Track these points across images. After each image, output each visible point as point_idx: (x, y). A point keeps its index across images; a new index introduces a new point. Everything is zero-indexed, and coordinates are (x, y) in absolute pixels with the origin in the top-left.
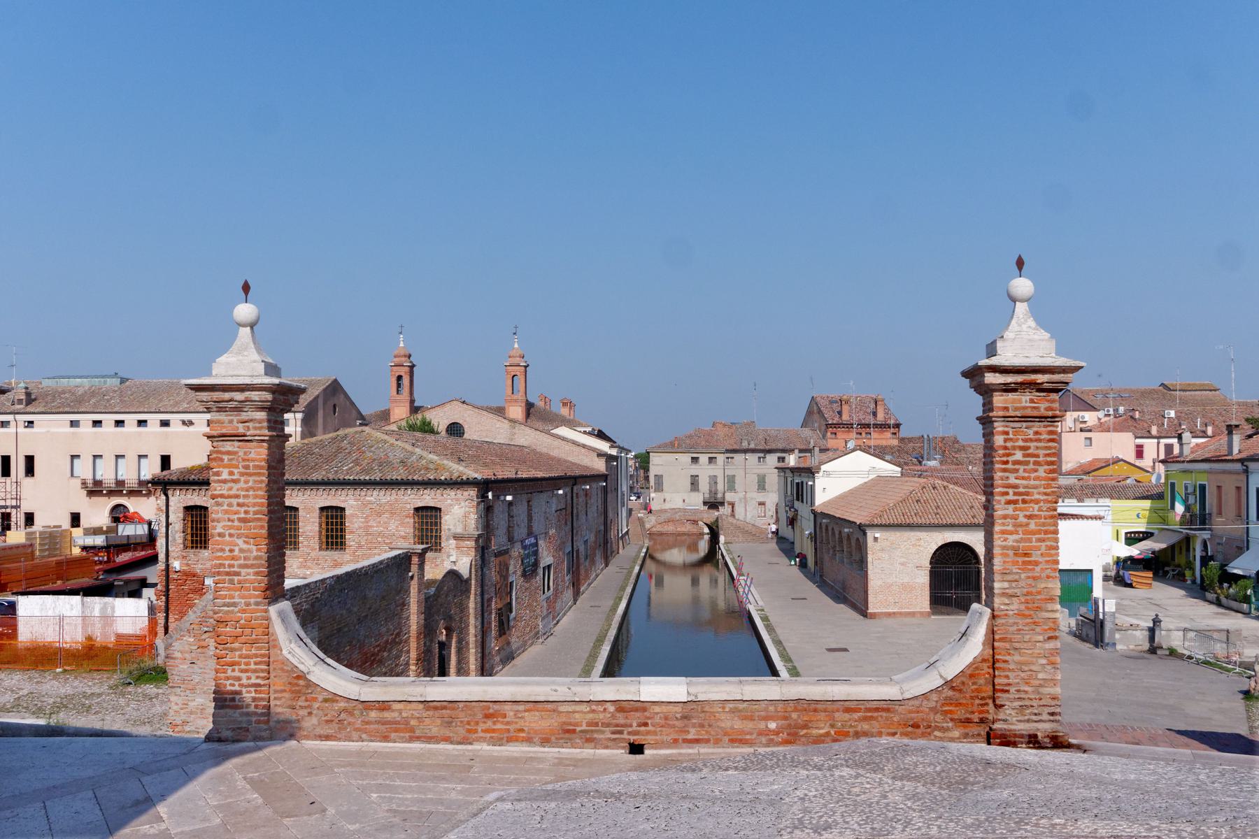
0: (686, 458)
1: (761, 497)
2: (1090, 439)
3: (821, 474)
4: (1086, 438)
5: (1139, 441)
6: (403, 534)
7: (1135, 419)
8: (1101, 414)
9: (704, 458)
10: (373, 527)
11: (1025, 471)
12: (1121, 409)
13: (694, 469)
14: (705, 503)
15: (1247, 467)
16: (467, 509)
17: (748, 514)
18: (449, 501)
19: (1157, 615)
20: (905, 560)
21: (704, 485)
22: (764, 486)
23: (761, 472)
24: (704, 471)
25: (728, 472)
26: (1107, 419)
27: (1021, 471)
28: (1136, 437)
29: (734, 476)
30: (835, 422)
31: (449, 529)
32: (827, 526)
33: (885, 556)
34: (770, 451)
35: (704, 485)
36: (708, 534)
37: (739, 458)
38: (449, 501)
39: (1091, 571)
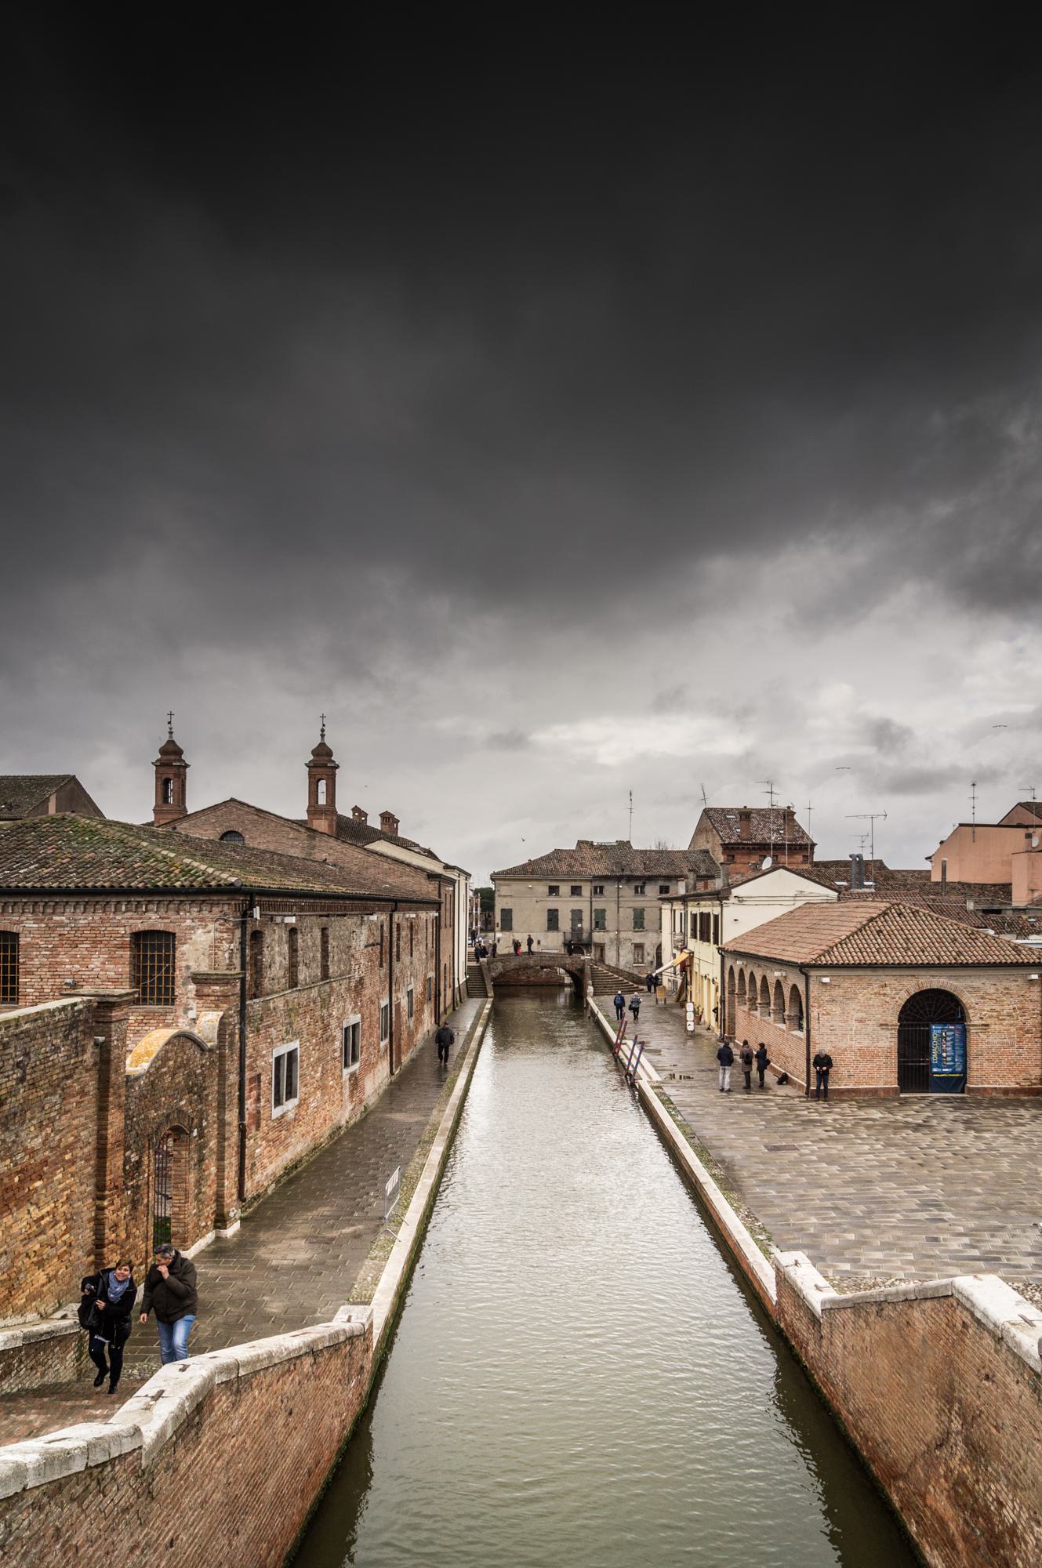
0: (542, 888)
1: (638, 938)
3: (732, 900)
6: (112, 974)
9: (565, 889)
10: (64, 964)
13: (553, 903)
16: (218, 935)
17: (621, 958)
18: (188, 922)
20: (863, 1015)
21: (565, 923)
22: (642, 923)
23: (639, 905)
24: (565, 905)
25: (596, 906)
29: (604, 910)
30: (732, 841)
31: (188, 967)
32: (741, 971)
33: (836, 1009)
35: (565, 923)
36: (569, 985)
37: (610, 888)
38: (188, 922)
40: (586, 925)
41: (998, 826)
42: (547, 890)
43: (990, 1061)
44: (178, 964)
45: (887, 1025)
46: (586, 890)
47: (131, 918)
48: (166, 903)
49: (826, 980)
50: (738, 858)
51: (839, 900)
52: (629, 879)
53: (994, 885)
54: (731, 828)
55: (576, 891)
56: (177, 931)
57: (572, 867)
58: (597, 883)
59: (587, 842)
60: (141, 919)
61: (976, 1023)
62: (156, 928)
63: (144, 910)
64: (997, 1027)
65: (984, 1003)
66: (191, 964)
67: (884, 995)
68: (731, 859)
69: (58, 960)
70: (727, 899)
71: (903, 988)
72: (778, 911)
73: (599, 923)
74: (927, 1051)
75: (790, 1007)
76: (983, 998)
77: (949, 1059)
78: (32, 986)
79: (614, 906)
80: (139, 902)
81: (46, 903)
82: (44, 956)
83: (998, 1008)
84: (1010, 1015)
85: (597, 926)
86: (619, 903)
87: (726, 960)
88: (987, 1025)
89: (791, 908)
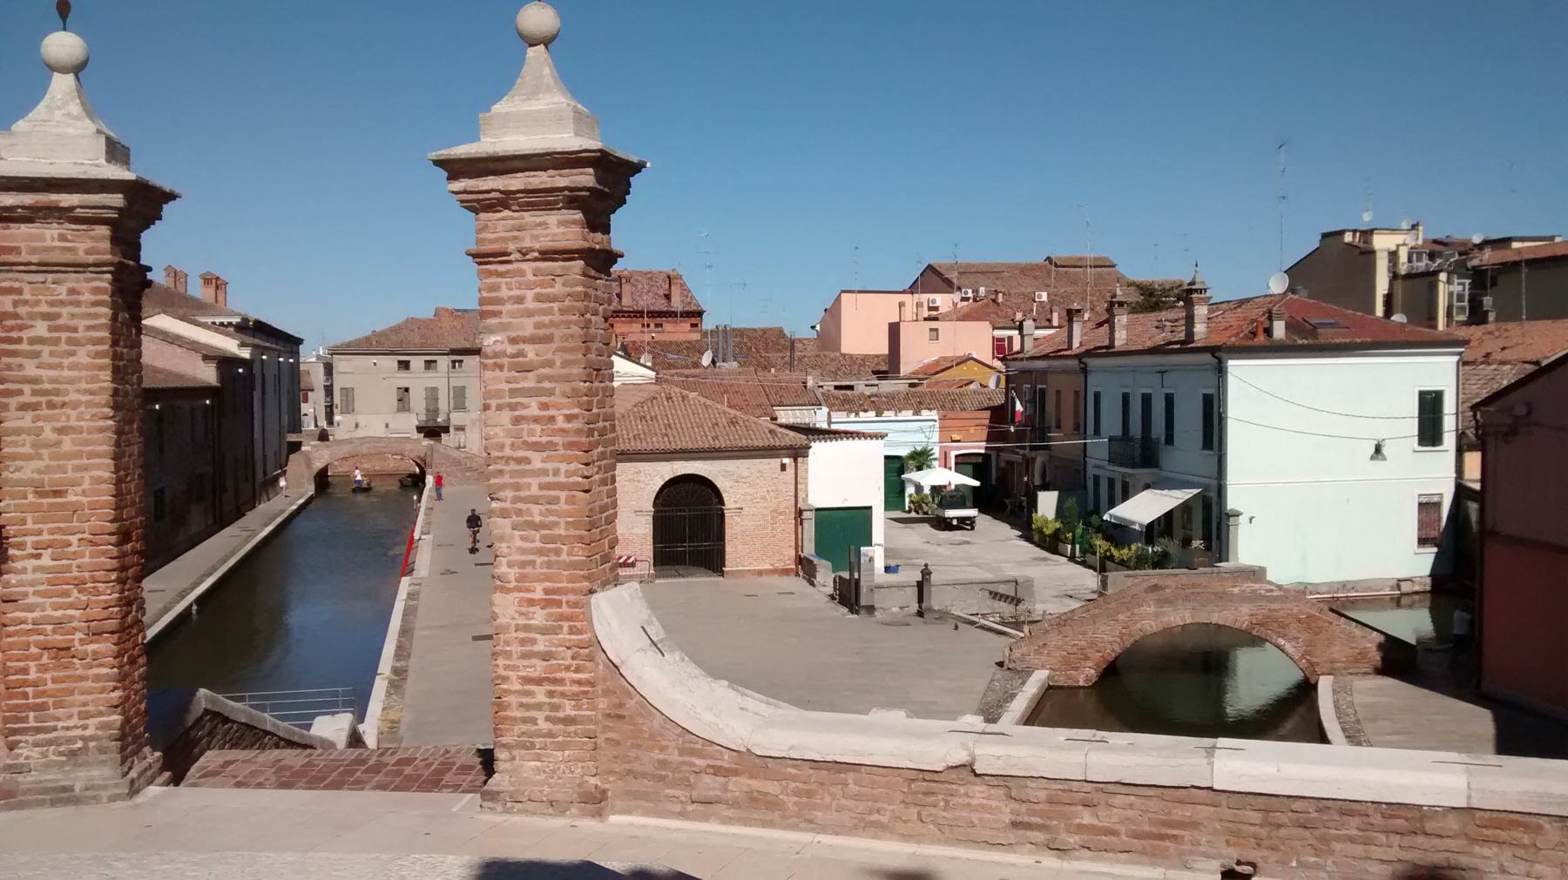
0: (391, 362)
2: (936, 330)
4: (931, 330)
7: (998, 304)
8: (956, 296)
9: (417, 363)
11: (52, 354)
12: (982, 290)
13: (404, 379)
15: (1086, 365)
19: (926, 565)
24: (418, 380)
25: (454, 383)
26: (965, 303)
27: (45, 355)
29: (464, 387)
39: (870, 508)
42: (396, 364)
55: (429, 365)
67: (639, 481)
73: (460, 403)
76: (737, 482)
84: (763, 498)
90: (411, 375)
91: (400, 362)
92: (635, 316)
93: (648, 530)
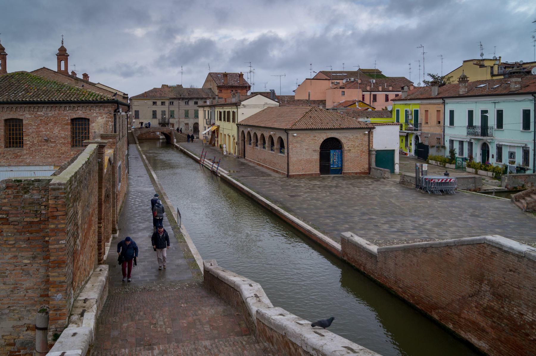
0: (150, 103)
1: (186, 121)
3: (241, 106)
5: (364, 93)
9: (159, 103)
13: (154, 108)
14: (159, 124)
15: (444, 101)
16: (107, 119)
18: (95, 114)
20: (308, 147)
21: (159, 116)
22: (188, 116)
23: (187, 109)
24: (159, 109)
25: (171, 109)
28: (363, 91)
29: (174, 111)
30: (221, 85)
31: (95, 132)
33: (298, 145)
34: (191, 99)
35: (159, 116)
37: (176, 102)
38: (95, 114)
40: (167, 116)
41: (313, 79)
42: (152, 103)
43: (351, 163)
44: (91, 131)
45: (316, 150)
46: (167, 103)
47: (71, 113)
48: (85, 107)
49: (295, 135)
50: (223, 91)
51: (280, 106)
52: (183, 99)
53: (318, 101)
54: (220, 80)
55: (163, 103)
56: (90, 118)
57: (161, 94)
58: (171, 101)
59: (166, 85)
60: (75, 113)
61: (346, 149)
62: (81, 117)
63: (76, 109)
64: (353, 150)
65: (349, 142)
66: (96, 131)
67: (315, 140)
68: (220, 91)
69: (40, 130)
70: (240, 106)
71: (322, 137)
72: (257, 110)
73: (172, 116)
74: (329, 160)
75: (277, 145)
76: (349, 140)
77: (336, 162)
78: (29, 141)
79: (178, 109)
80: (74, 106)
81: (34, 107)
82: (34, 128)
83: (354, 144)
84: (358, 146)
85: (171, 117)
86: (180, 108)
87: (240, 128)
88: (350, 150)
89: (263, 109)
90: (157, 107)
91: (153, 102)
92: (229, 88)
93: (318, 157)
